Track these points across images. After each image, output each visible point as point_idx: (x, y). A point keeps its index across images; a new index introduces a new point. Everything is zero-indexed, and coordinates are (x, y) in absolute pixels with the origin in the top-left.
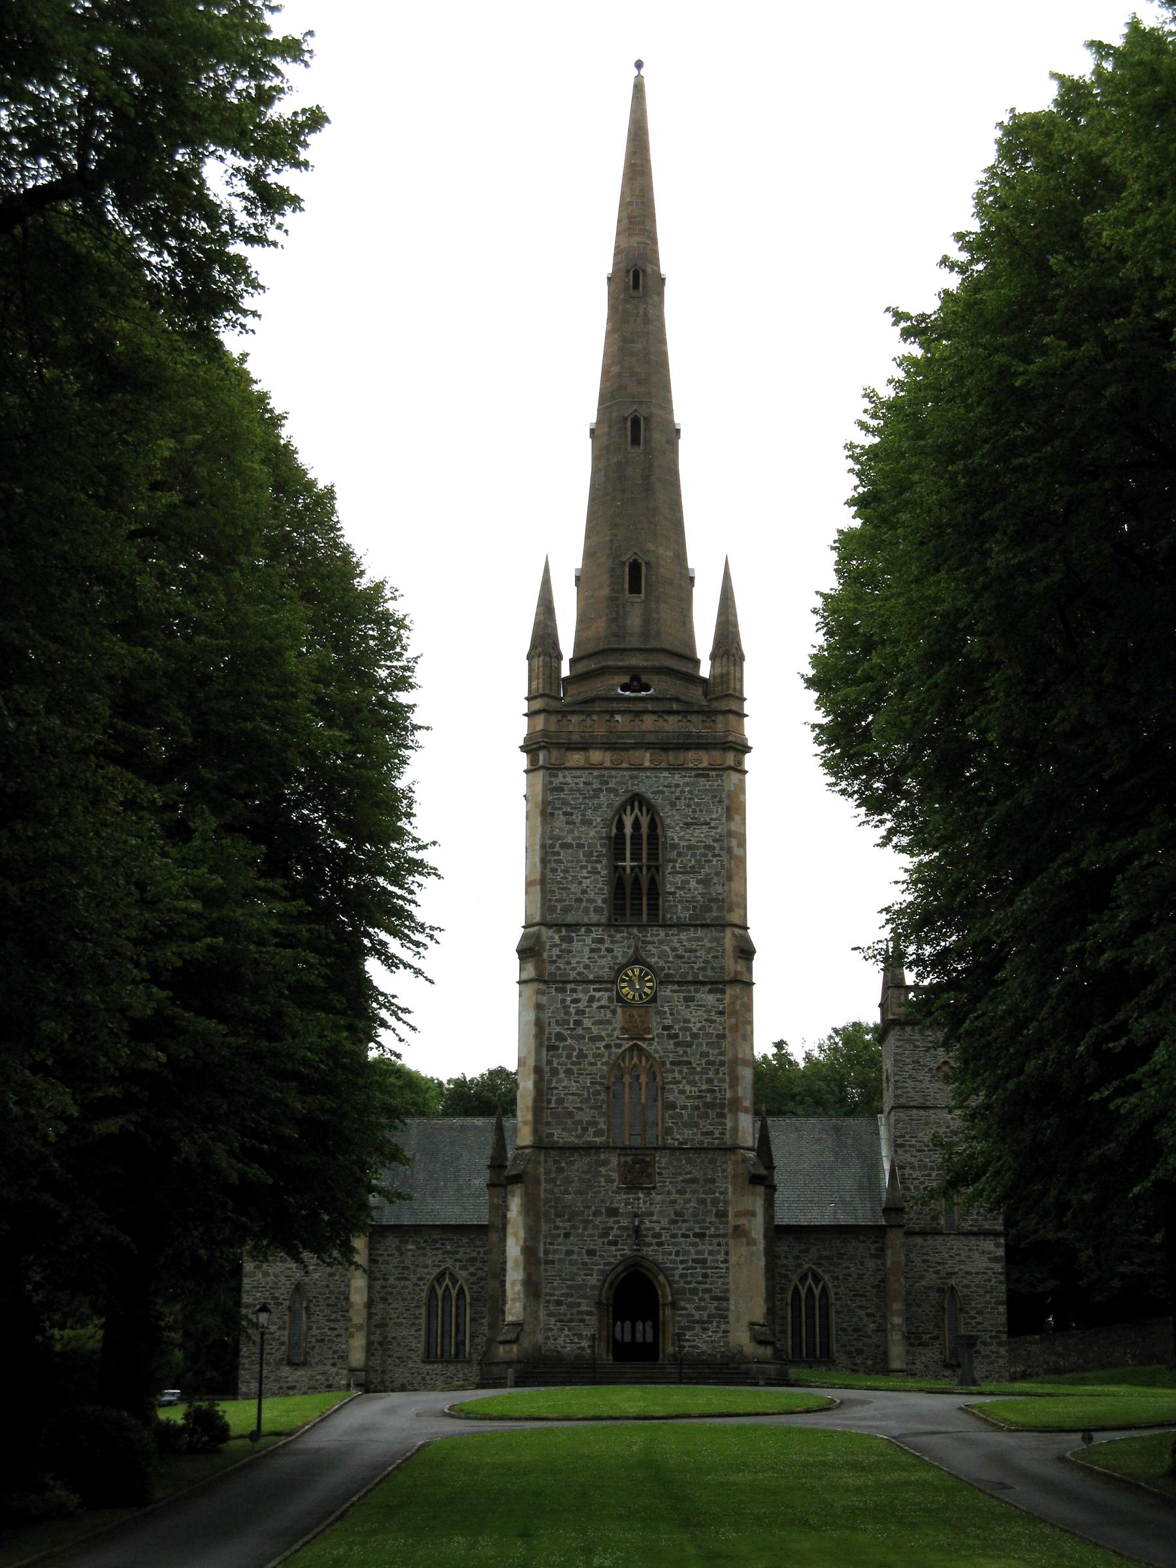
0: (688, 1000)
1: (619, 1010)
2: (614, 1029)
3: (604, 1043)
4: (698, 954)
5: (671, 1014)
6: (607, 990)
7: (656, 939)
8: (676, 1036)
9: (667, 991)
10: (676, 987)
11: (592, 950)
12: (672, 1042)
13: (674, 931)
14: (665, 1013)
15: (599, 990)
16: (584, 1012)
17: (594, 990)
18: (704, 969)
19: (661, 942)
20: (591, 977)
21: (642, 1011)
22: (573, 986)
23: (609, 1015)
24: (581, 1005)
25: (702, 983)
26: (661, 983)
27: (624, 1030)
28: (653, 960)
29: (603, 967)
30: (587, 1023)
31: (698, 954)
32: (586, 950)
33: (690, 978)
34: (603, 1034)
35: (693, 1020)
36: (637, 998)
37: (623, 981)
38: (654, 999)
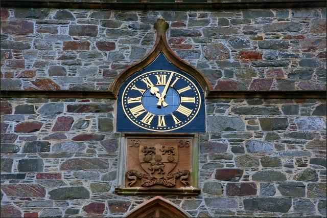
0: (268, 126)
1: (123, 143)
2: (114, 176)
3: (86, 202)
4: (290, 51)
5: (234, 150)
6: (97, 110)
7: (201, 29)
8: (249, 189)
9: (228, 110)
10: (245, 104)
11: (68, 46)
12: (239, 200)
13: (241, 15)
14: (224, 147)
15: (81, 109)
16: (44, 147)
17: (70, 109)
18: (302, 74)
19: (211, 34)
20: (66, 87)
21: (174, 144)
22: (24, 102)
23: (100, 150)
24: (39, 136)
25: (302, 96)
26: (213, 95)
27: (131, 177)
28: (194, 62)
29: (91, 72)
30: (50, 165)
31: (290, 51)
32: (57, 50)
33: (275, 86)
34: (86, 185)
35: (284, 161)
36: (162, 122)
37: (135, 94)
38: (199, 124)
